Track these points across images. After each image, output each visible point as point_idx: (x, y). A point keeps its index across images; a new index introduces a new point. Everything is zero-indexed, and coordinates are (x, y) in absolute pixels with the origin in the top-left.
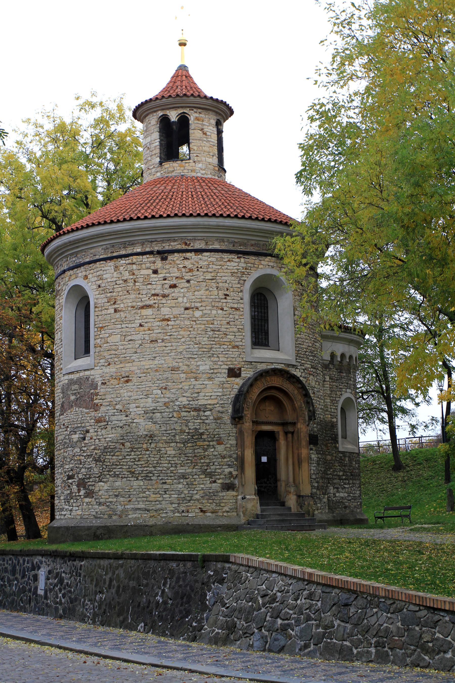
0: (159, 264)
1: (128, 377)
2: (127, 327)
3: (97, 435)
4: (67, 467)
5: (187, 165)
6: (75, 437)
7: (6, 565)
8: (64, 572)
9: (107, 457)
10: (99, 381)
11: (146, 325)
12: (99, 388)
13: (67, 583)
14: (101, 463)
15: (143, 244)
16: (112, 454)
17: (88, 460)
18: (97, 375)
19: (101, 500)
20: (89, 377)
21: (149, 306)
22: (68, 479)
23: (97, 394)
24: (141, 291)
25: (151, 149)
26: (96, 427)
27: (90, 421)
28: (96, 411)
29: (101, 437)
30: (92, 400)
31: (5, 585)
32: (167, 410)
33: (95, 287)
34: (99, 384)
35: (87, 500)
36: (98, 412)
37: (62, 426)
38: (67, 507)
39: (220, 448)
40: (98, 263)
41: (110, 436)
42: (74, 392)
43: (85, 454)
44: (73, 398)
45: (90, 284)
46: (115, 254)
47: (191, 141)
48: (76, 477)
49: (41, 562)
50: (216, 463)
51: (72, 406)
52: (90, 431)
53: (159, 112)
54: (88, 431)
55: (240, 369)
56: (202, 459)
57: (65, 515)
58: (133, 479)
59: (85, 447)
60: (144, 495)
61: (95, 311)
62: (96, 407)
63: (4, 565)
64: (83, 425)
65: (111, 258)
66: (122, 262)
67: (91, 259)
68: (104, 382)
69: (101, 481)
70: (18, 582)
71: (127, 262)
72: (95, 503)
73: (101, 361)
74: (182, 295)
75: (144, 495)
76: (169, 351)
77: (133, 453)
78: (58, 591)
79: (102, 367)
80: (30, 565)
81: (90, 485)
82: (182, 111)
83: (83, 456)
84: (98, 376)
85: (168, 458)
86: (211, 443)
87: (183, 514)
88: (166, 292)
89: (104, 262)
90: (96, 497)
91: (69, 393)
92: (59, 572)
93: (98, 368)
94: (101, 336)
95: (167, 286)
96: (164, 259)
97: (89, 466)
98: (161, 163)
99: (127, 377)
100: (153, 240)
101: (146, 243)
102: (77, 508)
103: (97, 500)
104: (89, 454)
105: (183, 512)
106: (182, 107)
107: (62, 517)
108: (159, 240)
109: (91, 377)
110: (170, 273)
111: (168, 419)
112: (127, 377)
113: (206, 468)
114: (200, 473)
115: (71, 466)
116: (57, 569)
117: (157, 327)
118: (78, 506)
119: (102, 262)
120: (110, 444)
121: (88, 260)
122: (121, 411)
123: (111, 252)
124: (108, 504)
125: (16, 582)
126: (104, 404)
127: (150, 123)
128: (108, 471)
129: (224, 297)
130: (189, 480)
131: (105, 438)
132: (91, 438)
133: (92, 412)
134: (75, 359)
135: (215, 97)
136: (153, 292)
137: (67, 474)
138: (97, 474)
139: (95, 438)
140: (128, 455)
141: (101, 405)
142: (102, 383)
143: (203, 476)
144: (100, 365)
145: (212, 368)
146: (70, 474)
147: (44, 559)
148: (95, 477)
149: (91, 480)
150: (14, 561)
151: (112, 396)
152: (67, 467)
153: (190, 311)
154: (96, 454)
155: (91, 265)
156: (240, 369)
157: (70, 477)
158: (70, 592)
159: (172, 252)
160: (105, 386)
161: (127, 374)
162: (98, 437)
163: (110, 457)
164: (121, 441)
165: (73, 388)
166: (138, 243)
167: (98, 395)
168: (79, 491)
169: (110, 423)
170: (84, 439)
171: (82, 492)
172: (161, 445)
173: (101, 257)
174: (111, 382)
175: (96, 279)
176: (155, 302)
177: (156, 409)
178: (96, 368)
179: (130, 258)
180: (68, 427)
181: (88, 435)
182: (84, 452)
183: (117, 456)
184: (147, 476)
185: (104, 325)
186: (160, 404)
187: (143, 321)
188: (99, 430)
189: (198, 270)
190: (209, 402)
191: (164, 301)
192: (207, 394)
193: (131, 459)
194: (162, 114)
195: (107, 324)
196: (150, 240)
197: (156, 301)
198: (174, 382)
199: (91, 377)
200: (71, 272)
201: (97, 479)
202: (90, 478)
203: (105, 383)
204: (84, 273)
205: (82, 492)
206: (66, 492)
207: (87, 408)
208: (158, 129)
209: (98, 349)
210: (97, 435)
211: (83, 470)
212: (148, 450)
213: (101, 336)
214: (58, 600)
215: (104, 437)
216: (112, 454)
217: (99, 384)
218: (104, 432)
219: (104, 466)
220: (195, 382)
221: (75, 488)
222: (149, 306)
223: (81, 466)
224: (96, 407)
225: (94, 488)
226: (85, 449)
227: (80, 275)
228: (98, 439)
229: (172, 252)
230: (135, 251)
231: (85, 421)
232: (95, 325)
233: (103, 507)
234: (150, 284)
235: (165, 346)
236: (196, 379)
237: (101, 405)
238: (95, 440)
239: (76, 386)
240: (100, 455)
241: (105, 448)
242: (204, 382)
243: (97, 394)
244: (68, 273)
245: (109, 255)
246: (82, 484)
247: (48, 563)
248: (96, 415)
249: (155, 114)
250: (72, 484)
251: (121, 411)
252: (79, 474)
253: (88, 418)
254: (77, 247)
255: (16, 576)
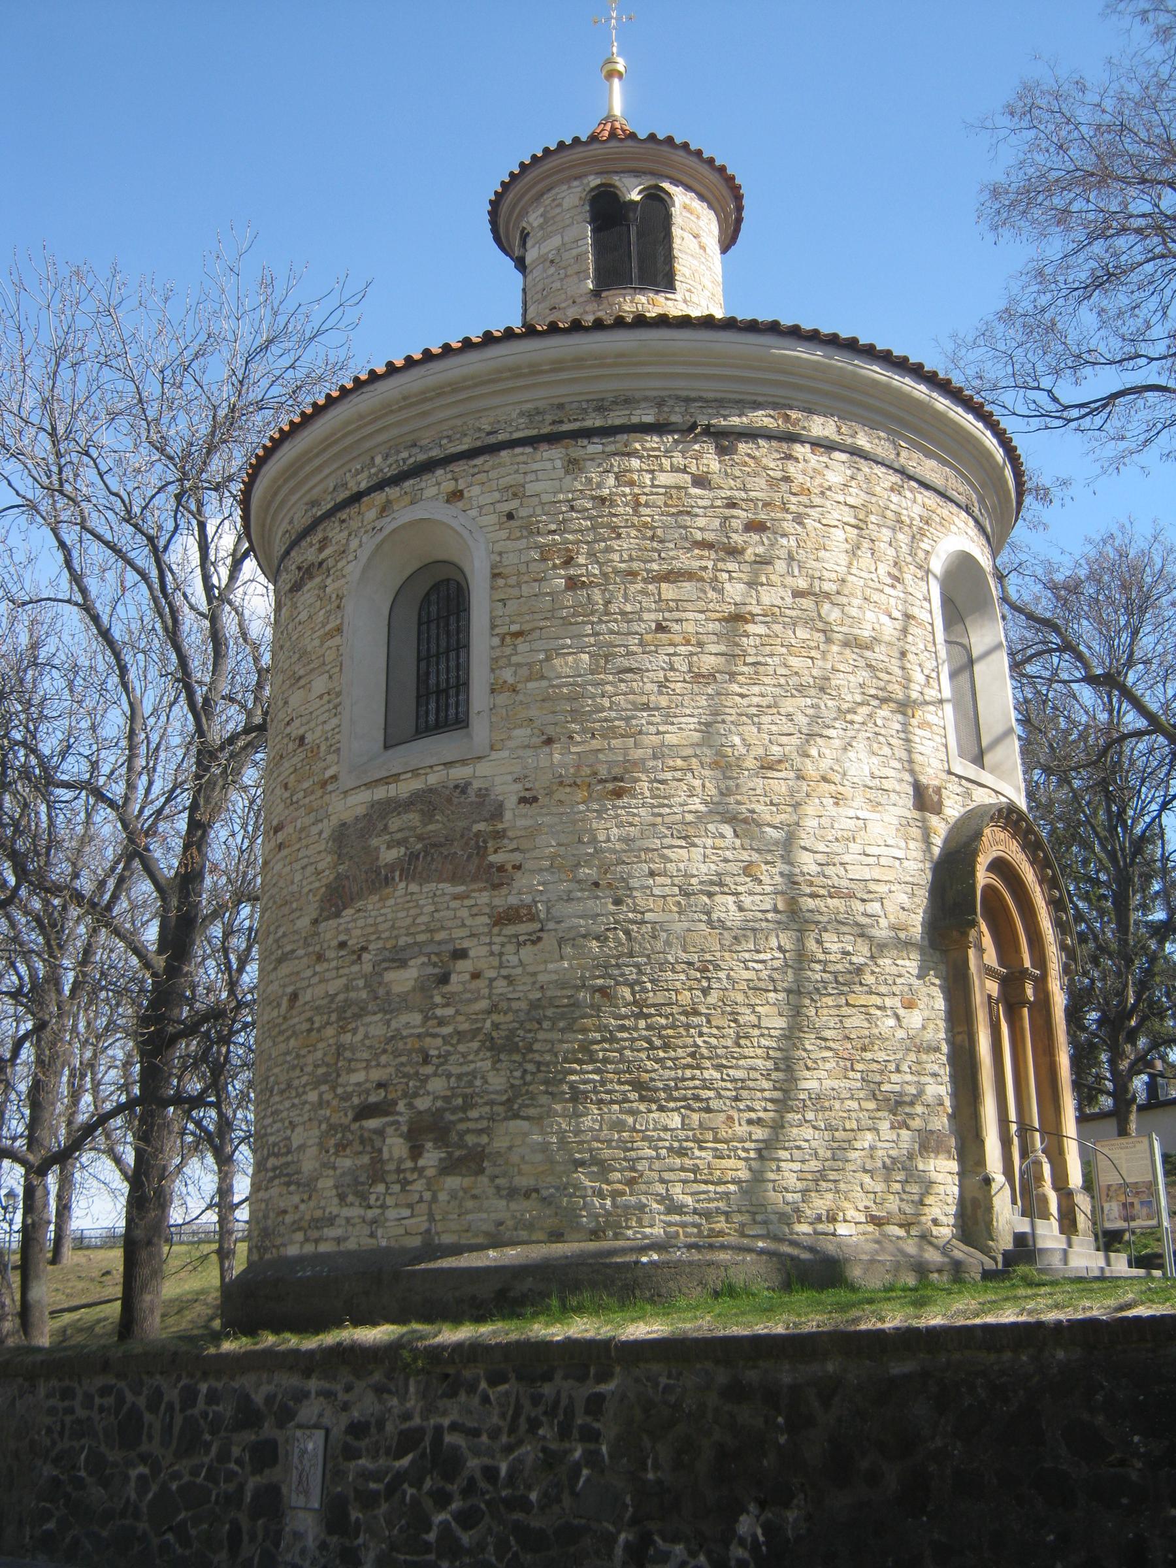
0: (711, 462)
1: (622, 780)
2: (612, 632)
3: (501, 966)
4: (359, 1077)
5: (669, 303)
6: (403, 980)
7: (81, 1413)
8: (454, 1427)
9: (541, 1035)
10: (507, 792)
11: (676, 627)
12: (508, 815)
13: (490, 1473)
14: (517, 1057)
15: (660, 403)
16: (561, 1024)
17: (462, 1048)
18: (497, 774)
19: (523, 1182)
20: (470, 784)
21: (689, 575)
22: (356, 1118)
23: (499, 835)
24: (659, 532)
25: (563, 264)
26: (497, 939)
27: (467, 923)
28: (496, 887)
29: (519, 970)
30: (482, 852)
31: (79, 1483)
32: (758, 889)
33: (492, 519)
34: (511, 802)
35: (453, 1182)
36: (504, 890)
37: (330, 954)
38: (355, 1212)
39: (914, 1019)
40: (504, 453)
41: (551, 966)
42: (399, 836)
43: (447, 1030)
44: (390, 855)
45: (473, 513)
46: (566, 427)
47: (676, 253)
48: (401, 1106)
49: (301, 1396)
50: (905, 1068)
51: (388, 881)
52: (472, 953)
53: (591, 178)
54: (461, 954)
55: (938, 790)
56: (864, 1049)
57: (339, 1240)
58: (642, 1107)
59: (447, 1005)
60: (688, 1162)
61: (492, 588)
62: (498, 877)
63: (70, 1411)
64: (439, 937)
65: (552, 439)
66: (591, 449)
67: (479, 444)
68: (527, 794)
69: (516, 1116)
70: (156, 1468)
71: (610, 448)
72: (491, 1191)
73: (517, 732)
74: (783, 553)
75: (688, 1162)
76: (754, 710)
77: (642, 1024)
78: (428, 1503)
79: (520, 752)
80: (226, 1409)
81: (468, 1131)
82: (652, 182)
83: (434, 1036)
84: (510, 778)
85: (763, 1042)
86: (889, 1002)
87: (821, 1227)
88: (737, 539)
89: (528, 450)
90: (497, 1171)
91: (374, 842)
92: (421, 1430)
93: (505, 754)
94: (514, 659)
95: (737, 524)
96: (722, 451)
97: (465, 1069)
98: (596, 294)
99: (615, 779)
100: (693, 394)
101: (671, 402)
102: (406, 1212)
103: (500, 1181)
104: (465, 1026)
105: (819, 1219)
106: (653, 174)
107: (323, 1248)
108: (711, 395)
109: (476, 784)
110: (745, 490)
111: (760, 915)
112: (615, 779)
113: (878, 1078)
114: (862, 1094)
115: (376, 1075)
116: (407, 1416)
117: (714, 638)
118: (410, 1206)
119: (518, 450)
120: (549, 993)
121: (465, 447)
122: (597, 885)
123: (554, 422)
124: (545, 1193)
125: (142, 1469)
126: (528, 865)
127: (559, 205)
128: (547, 1082)
129: (889, 581)
130: (833, 1114)
131: (534, 974)
132: (476, 976)
133: (481, 890)
134: (387, 747)
135: (729, 172)
136: (698, 536)
137: (356, 1100)
138: (497, 1092)
139: (492, 974)
140: (623, 1028)
141: (518, 867)
142: (523, 800)
143: (872, 1105)
144: (510, 744)
145: (877, 773)
146: (373, 1099)
147: (313, 1384)
148: (492, 1103)
149: (473, 1114)
150: (129, 1397)
151: (564, 839)
152: (359, 1077)
153: (807, 603)
154: (496, 1026)
155: (478, 461)
156: (938, 790)
157: (365, 1111)
158: (523, 1504)
159: (751, 435)
160: (533, 809)
161: (617, 771)
162: (504, 972)
163: (557, 1036)
164: (600, 982)
165: (395, 823)
166: (646, 399)
167: (504, 837)
168: (416, 1152)
169: (551, 925)
170: (444, 979)
171: (431, 1157)
172: (740, 998)
173: (516, 435)
174: (556, 796)
175: (497, 495)
176: (704, 563)
177: (721, 884)
178: (494, 755)
179: (619, 437)
180: (364, 949)
181: (461, 965)
182: (441, 1022)
183: (584, 1030)
184: (697, 1098)
185: (527, 627)
186: (733, 868)
187: (667, 615)
188: (511, 948)
189: (822, 493)
190: (876, 873)
191: (732, 566)
192: (869, 850)
193: (633, 1040)
194: (598, 182)
195: (542, 624)
196: (684, 394)
197: (710, 564)
198: (772, 804)
199: (476, 784)
200: (392, 492)
201: (499, 1109)
202: (464, 1108)
203: (535, 799)
204: (449, 486)
205: (431, 1157)
206: (346, 1163)
207: (454, 879)
208: (587, 216)
209: (502, 699)
210: (501, 966)
211: (437, 1085)
212: (696, 1013)
213: (514, 659)
214: (431, 1537)
215: (530, 969)
216: (561, 1024)
217: (511, 802)
218: (527, 953)
219: (530, 1067)
220: (832, 810)
221: (395, 1147)
222: (689, 575)
223: (429, 1070)
224: (498, 877)
225: (485, 1139)
226: (450, 1011)
227: (431, 491)
228: (505, 977)
229: (751, 435)
230: (635, 420)
231: (449, 924)
232: (493, 627)
233: (527, 1204)
234: (688, 513)
235: (742, 696)
236: (838, 799)
237: (518, 867)
238: (492, 980)
239: (411, 816)
240: (512, 1032)
241: (535, 1005)
242: (860, 814)
243: (499, 835)
244: (379, 498)
245: (546, 430)
246: (427, 1129)
247: (342, 1397)
248: (496, 902)
249: (576, 183)
250: (380, 1132)
251: (597, 885)
252: (416, 1095)
253: (464, 913)
254: (424, 414)
255: (144, 1448)
